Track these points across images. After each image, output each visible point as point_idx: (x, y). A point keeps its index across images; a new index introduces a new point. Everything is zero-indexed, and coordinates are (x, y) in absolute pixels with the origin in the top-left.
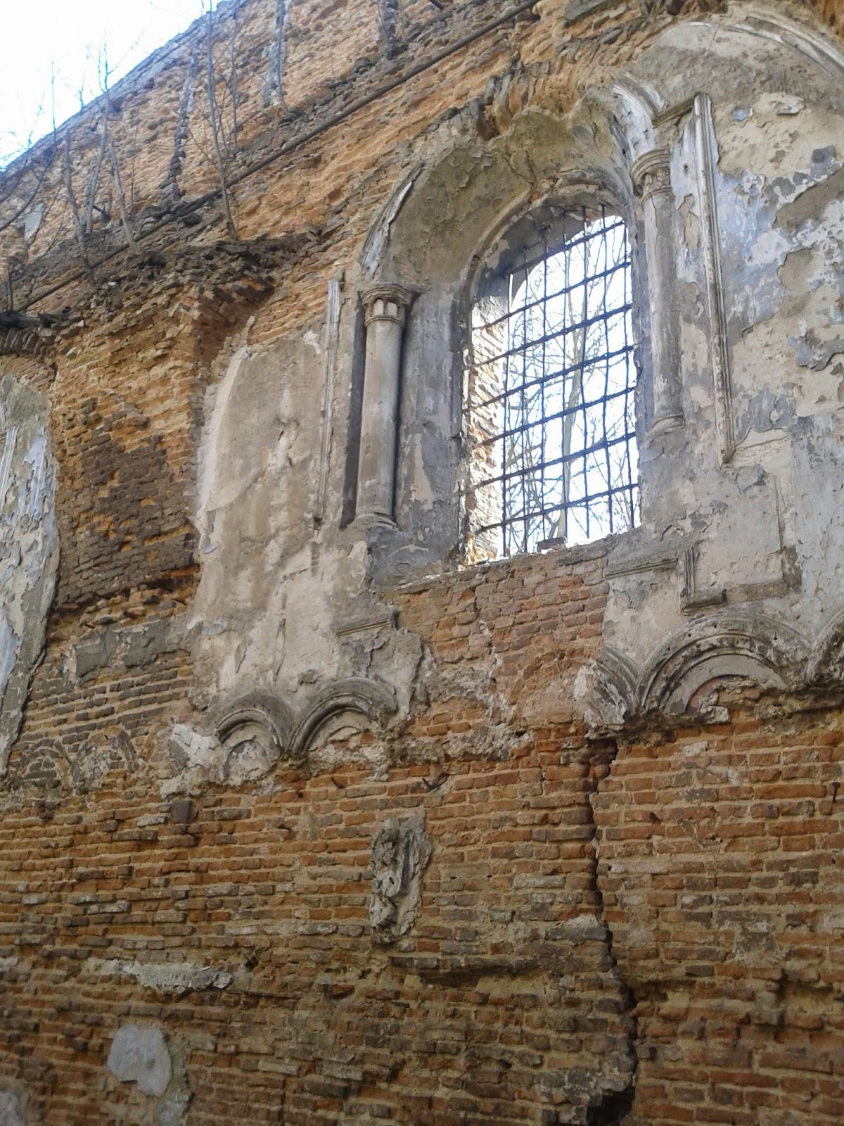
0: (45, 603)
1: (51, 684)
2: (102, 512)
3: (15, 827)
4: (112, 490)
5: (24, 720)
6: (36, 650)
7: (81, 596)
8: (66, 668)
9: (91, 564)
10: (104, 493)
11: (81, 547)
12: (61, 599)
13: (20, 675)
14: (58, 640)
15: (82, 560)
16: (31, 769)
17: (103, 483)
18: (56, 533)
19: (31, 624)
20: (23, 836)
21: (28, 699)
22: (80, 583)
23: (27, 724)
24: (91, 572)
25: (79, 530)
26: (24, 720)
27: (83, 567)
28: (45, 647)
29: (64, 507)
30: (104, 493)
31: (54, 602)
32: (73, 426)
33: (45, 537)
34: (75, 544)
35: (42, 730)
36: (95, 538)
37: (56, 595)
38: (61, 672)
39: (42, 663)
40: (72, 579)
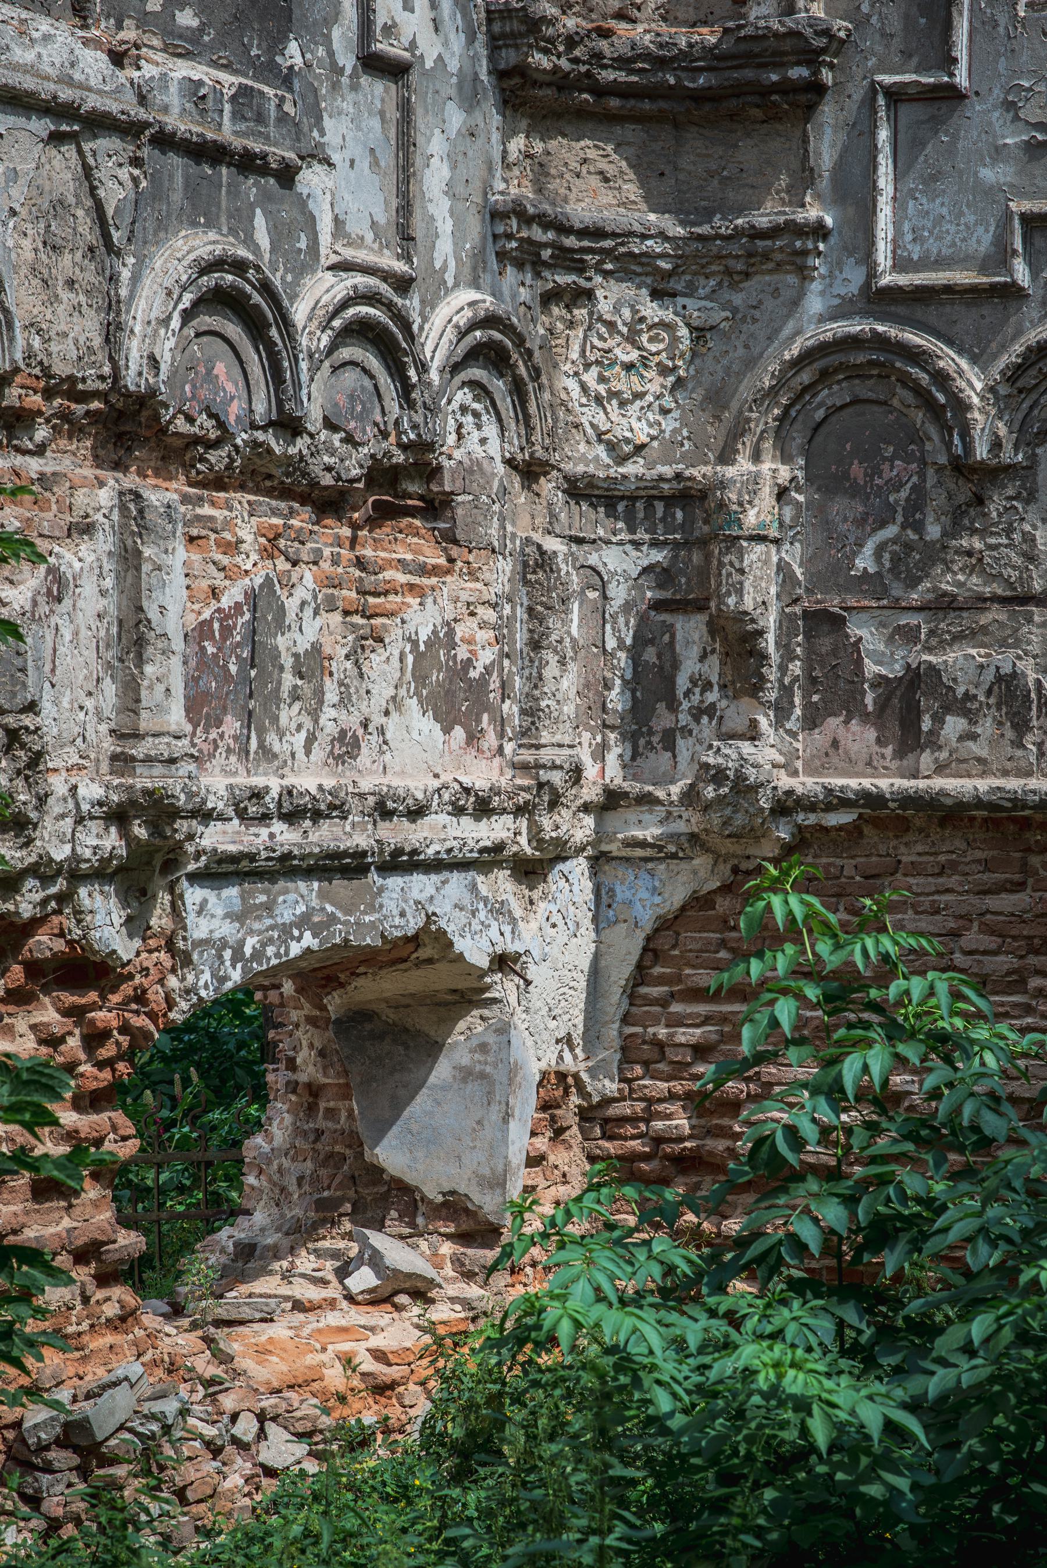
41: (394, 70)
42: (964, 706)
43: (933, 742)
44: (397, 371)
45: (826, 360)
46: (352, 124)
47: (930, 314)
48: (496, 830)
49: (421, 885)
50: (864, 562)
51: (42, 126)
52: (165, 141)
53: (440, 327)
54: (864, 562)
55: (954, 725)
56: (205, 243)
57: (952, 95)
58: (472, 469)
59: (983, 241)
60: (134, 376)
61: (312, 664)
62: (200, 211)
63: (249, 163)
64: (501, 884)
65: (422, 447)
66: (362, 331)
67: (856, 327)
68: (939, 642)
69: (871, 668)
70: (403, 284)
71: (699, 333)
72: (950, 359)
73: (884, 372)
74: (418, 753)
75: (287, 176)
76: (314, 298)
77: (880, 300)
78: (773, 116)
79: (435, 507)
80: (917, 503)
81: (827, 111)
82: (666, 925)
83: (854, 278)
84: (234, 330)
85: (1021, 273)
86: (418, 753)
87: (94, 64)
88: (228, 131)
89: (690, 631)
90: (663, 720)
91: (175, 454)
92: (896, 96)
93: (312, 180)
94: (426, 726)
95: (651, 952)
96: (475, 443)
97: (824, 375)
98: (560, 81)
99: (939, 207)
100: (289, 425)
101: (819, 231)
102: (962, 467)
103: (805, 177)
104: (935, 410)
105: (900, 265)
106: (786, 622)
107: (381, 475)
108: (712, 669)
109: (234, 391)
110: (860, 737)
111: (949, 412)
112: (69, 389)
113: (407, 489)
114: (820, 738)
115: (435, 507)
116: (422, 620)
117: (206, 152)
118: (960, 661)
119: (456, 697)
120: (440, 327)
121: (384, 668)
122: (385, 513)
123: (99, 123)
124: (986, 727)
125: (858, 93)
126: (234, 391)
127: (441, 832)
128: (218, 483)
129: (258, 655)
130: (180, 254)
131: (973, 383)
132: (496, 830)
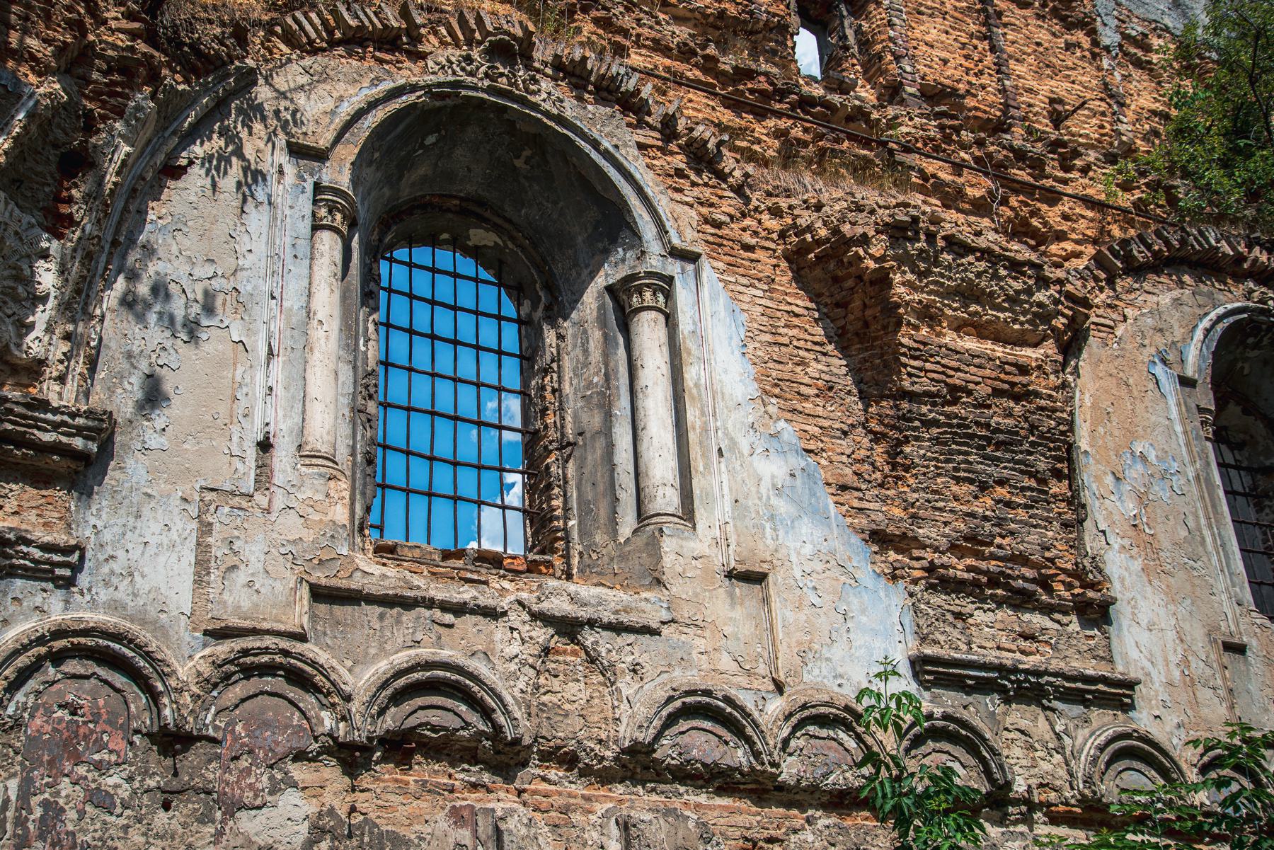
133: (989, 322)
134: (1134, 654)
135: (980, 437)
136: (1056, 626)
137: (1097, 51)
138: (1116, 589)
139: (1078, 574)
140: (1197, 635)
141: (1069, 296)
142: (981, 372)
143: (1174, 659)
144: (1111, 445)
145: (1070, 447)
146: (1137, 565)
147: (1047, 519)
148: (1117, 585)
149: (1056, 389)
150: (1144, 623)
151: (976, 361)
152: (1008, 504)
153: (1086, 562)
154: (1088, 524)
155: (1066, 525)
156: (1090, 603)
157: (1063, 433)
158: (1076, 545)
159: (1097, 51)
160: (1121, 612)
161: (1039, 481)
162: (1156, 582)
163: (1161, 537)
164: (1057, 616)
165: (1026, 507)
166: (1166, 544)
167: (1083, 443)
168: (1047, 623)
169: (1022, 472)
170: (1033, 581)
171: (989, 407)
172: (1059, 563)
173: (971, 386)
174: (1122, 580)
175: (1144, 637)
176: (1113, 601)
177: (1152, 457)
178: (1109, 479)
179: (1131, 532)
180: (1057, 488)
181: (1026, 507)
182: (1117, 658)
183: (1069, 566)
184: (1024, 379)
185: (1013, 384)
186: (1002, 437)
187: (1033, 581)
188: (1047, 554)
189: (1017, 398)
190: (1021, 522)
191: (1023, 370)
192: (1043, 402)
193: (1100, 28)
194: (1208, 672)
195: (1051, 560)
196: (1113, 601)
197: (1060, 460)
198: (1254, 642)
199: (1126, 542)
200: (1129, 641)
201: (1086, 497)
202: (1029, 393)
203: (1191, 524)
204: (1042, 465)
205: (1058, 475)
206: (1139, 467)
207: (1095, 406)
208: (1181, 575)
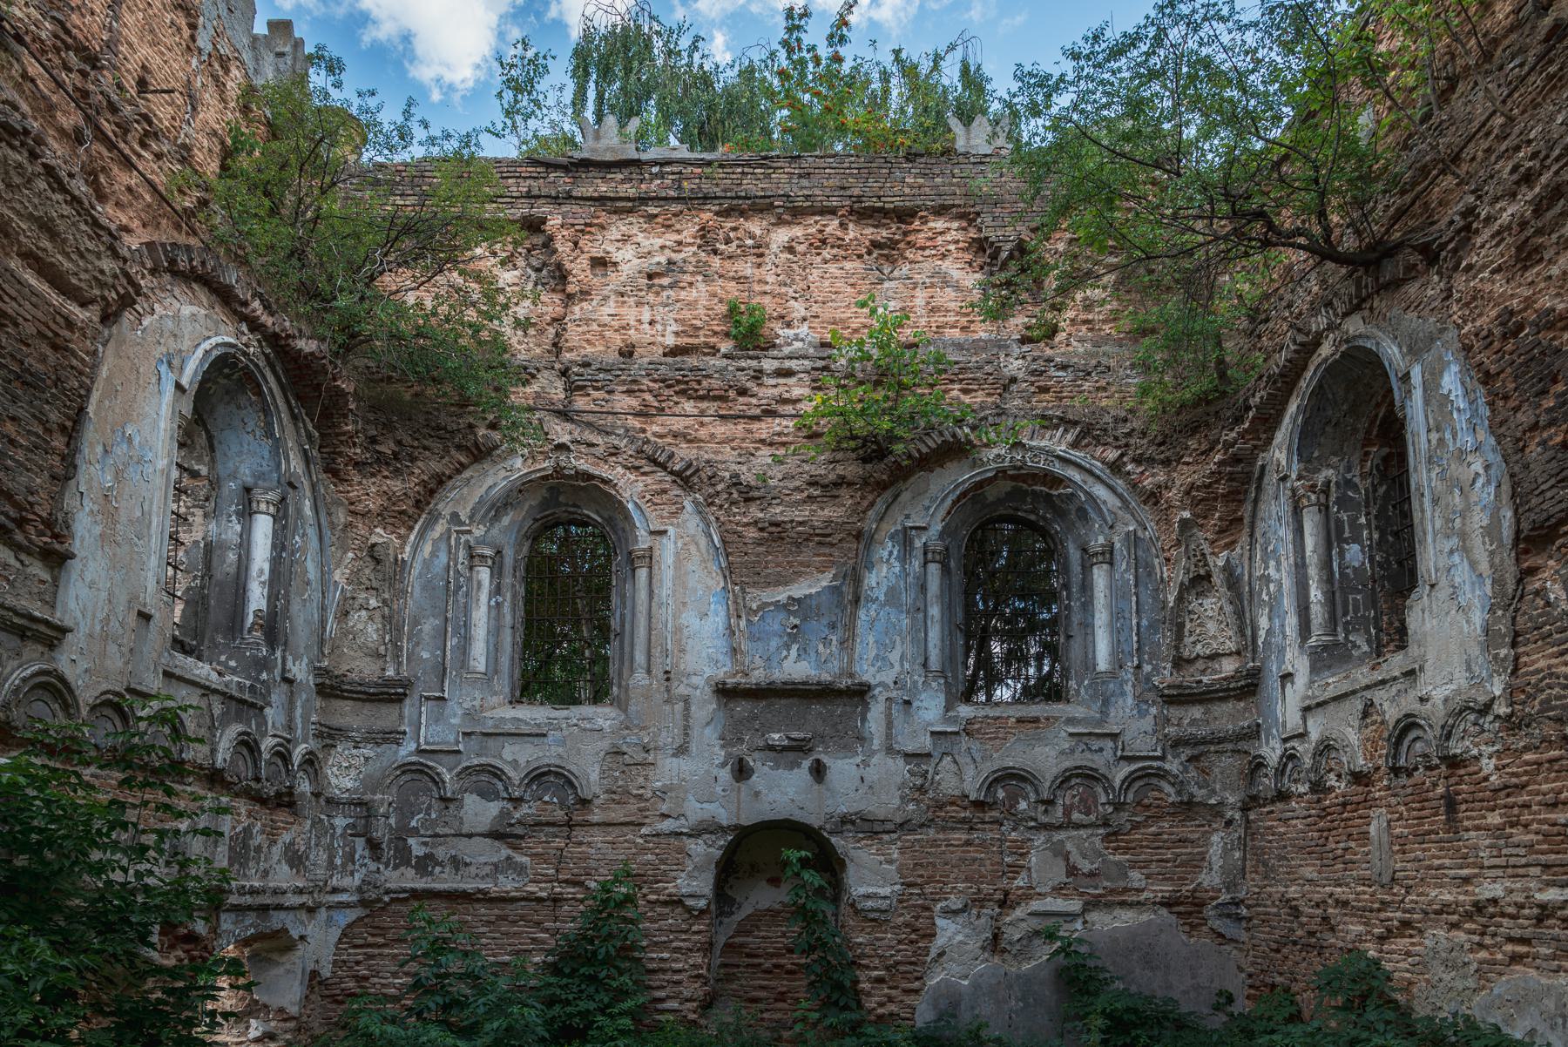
0: (1507, 532)
1: (1540, 615)
2: (1550, 424)
3: (1540, 764)
4: (1558, 396)
5: (1517, 659)
6: (1510, 588)
7: (1547, 519)
8: (1552, 596)
9: (1553, 481)
10: (1549, 403)
11: (1536, 470)
12: (1525, 526)
13: (1500, 613)
14: (1532, 571)
15: (1540, 480)
16: (1541, 703)
17: (1544, 392)
18: (1499, 458)
19: (1497, 561)
20: (1550, 770)
21: (1517, 634)
22: (1549, 504)
23: (1524, 659)
24: (1555, 490)
25: (1527, 450)
26: (1517, 659)
27: (1543, 487)
28: (1519, 581)
29: (1503, 429)
30: (1549, 403)
31: (1518, 532)
32: (1491, 343)
33: (1487, 468)
34: (1526, 467)
35: (1542, 664)
36: (1550, 454)
37: (1518, 522)
38: (1548, 604)
39: (1522, 597)
40: (1534, 501)
41: (290, 682)
42: (440, 864)
43: (431, 874)
44: (286, 766)
45: (405, 768)
46: (278, 696)
47: (435, 756)
48: (304, 899)
49: (282, 915)
50: (414, 823)
51: (200, 692)
52: (232, 697)
53: (297, 757)
54: (414, 823)
55: (438, 869)
56: (240, 728)
57: (443, 699)
58: (303, 794)
59: (452, 738)
60: (219, 763)
61: (258, 849)
62: (238, 718)
63: (253, 705)
64: (303, 915)
65: (291, 787)
66: (278, 754)
67: (414, 759)
68: (434, 846)
69: (415, 853)
70: (289, 741)
71: (367, 759)
72: (440, 769)
73: (421, 772)
74: (283, 877)
75: (262, 708)
76: (267, 743)
77: (420, 752)
78: (391, 701)
79: (291, 805)
80: (429, 807)
81: (408, 701)
82: (350, 926)
83: (413, 746)
84: (245, 752)
85: (461, 747)
86: (283, 877)
87: (214, 676)
88: (247, 697)
89: (360, 843)
90: (350, 867)
91: (227, 786)
92: (428, 698)
93: (268, 710)
94: (286, 868)
95: (344, 934)
96: (305, 787)
97: (403, 773)
98: (332, 687)
99: (439, 729)
100: (258, 780)
101: (404, 733)
102: (443, 799)
103: (401, 717)
104: (436, 783)
105: (427, 743)
106: (390, 841)
107: (279, 795)
108: (367, 853)
109: (244, 769)
110: (410, 872)
111: (437, 782)
112: (201, 767)
113: (286, 801)
114: (398, 873)
115: (291, 805)
116: (286, 837)
117: (242, 702)
118: (441, 853)
119: (296, 860)
120: (297, 757)
121: (277, 850)
122: (279, 805)
123: (215, 691)
124: (447, 870)
125: (416, 697)
126: (244, 769)
127: (292, 900)
128: (237, 795)
129: (245, 846)
130: (235, 729)
131: (447, 777)
132: (304, 899)
133: (53, 265)
134: (72, 605)
135: (11, 371)
136: (18, 565)
137: (191, 48)
138: (76, 546)
139: (49, 523)
140: (123, 598)
141: (127, 275)
142: (34, 311)
143: (100, 615)
144: (110, 419)
145: (82, 410)
146: (98, 530)
147: (40, 467)
148: (78, 542)
149: (87, 353)
150: (88, 580)
151: (34, 299)
152: (12, 442)
153: (60, 516)
154: (72, 483)
155: (53, 477)
156: (56, 552)
157: (80, 396)
158: (56, 499)
159: (191, 48)
160: (75, 566)
161: (48, 431)
162: (107, 549)
163: (122, 512)
164: (23, 557)
165: (28, 449)
166: (123, 519)
167: (91, 409)
168: (12, 561)
169: (34, 416)
170: (13, 520)
171: (28, 345)
172: (37, 509)
173: (20, 320)
174: (83, 540)
175: (84, 592)
176: (72, 556)
177: (136, 442)
178: (99, 449)
179: (101, 501)
180: (58, 442)
181: (28, 449)
182: (59, 605)
183: (44, 515)
184: (66, 333)
185: (57, 335)
186: (29, 379)
187: (13, 520)
188: (30, 498)
189: (55, 347)
190: (17, 461)
191: (70, 325)
192: (75, 362)
193: (200, 28)
194: (121, 631)
195: (32, 505)
196: (72, 556)
197: (69, 419)
198: (157, 615)
199: (96, 508)
200: (72, 592)
201: (79, 461)
202: (66, 349)
203: (146, 508)
204: (54, 416)
205: (63, 428)
206: (125, 446)
207: (108, 378)
208: (126, 548)
